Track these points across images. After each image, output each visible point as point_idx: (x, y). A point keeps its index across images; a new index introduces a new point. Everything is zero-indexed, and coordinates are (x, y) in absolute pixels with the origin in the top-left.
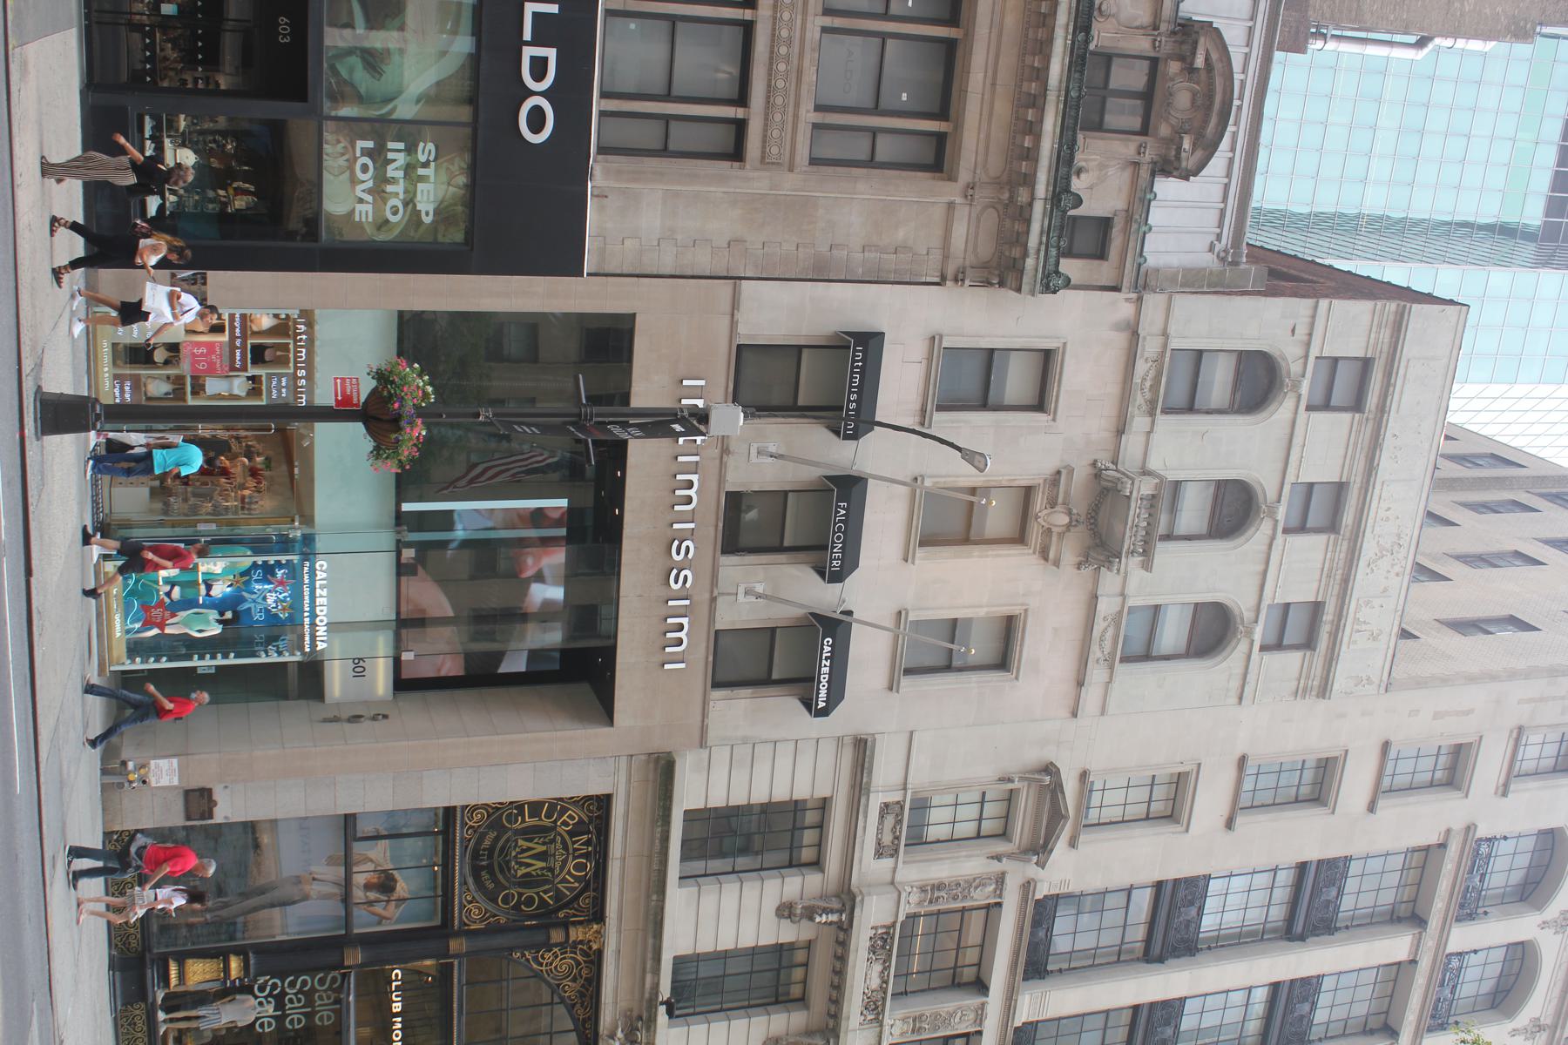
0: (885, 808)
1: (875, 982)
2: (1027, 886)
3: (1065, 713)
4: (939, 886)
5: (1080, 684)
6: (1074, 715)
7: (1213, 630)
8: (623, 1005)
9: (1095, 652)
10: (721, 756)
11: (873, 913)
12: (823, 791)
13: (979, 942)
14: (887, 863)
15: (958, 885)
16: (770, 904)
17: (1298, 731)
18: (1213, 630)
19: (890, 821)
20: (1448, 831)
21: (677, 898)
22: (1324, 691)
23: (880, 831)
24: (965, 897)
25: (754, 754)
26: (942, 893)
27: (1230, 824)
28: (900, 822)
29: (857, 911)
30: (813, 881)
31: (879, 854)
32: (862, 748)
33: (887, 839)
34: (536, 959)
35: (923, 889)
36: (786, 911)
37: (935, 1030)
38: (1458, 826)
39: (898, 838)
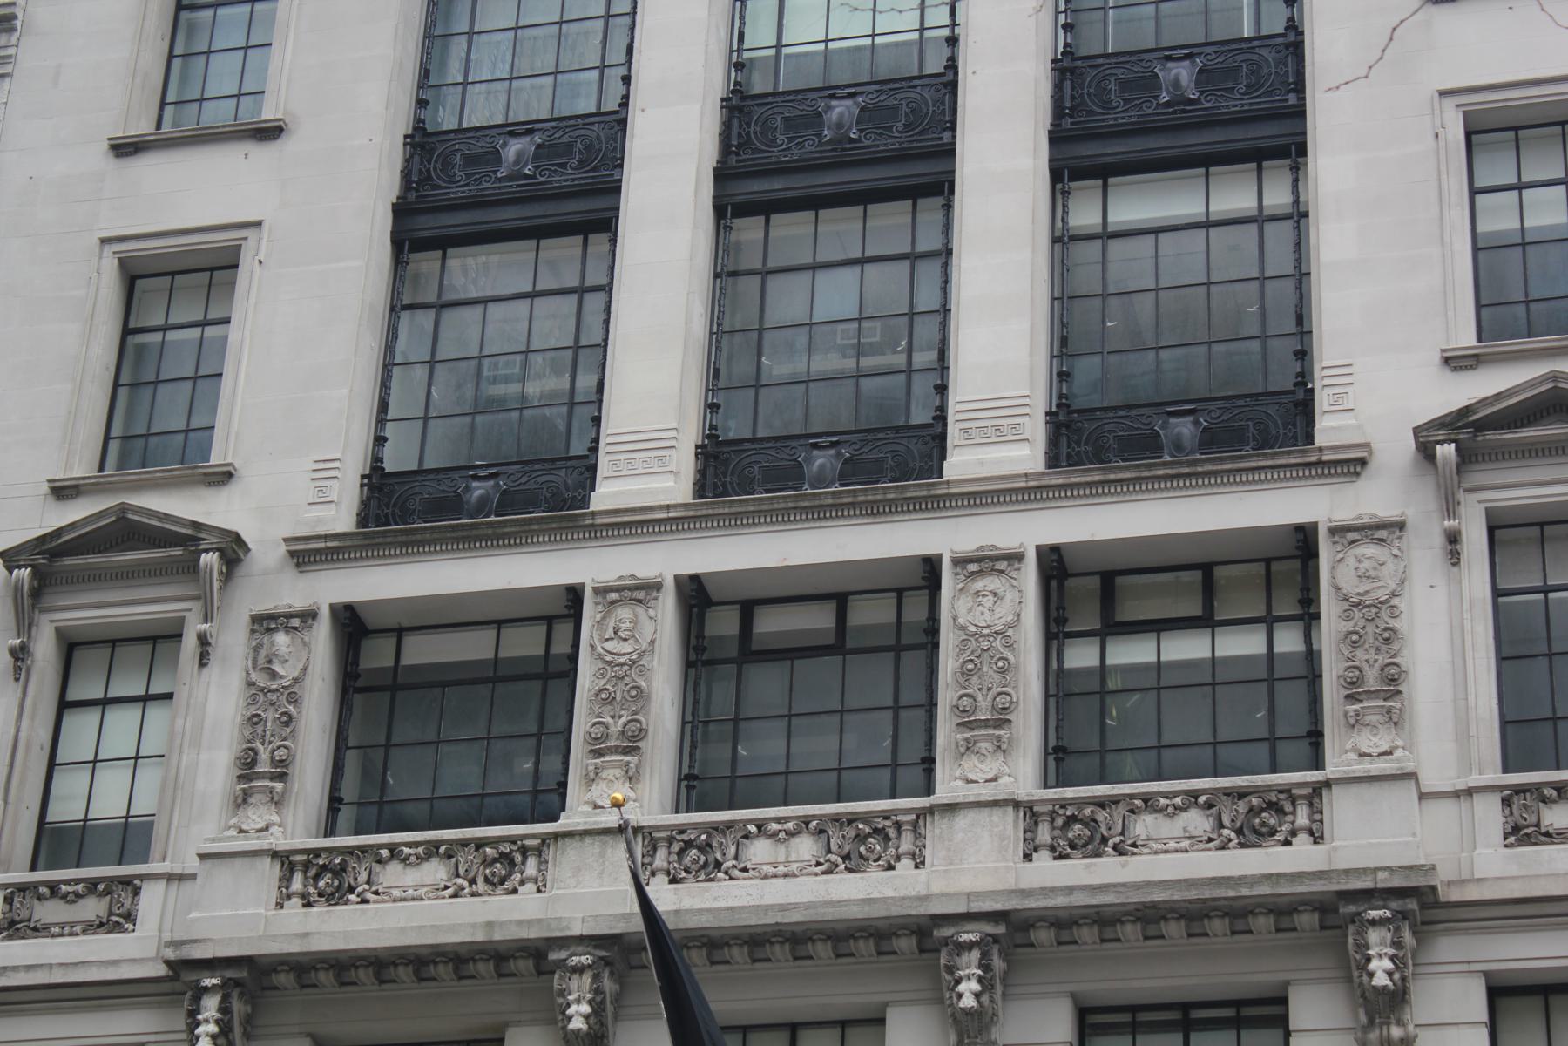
1: (435, 871)
2: (309, 554)
4: (247, 766)
11: (244, 915)
13: (489, 634)
14: (151, 899)
15: (254, 720)
19: (48, 912)
23: (65, 929)
24: (294, 699)
26: (264, 755)
28: (53, 887)
29: (198, 953)
31: (119, 921)
33: (93, 908)
37: (640, 696)
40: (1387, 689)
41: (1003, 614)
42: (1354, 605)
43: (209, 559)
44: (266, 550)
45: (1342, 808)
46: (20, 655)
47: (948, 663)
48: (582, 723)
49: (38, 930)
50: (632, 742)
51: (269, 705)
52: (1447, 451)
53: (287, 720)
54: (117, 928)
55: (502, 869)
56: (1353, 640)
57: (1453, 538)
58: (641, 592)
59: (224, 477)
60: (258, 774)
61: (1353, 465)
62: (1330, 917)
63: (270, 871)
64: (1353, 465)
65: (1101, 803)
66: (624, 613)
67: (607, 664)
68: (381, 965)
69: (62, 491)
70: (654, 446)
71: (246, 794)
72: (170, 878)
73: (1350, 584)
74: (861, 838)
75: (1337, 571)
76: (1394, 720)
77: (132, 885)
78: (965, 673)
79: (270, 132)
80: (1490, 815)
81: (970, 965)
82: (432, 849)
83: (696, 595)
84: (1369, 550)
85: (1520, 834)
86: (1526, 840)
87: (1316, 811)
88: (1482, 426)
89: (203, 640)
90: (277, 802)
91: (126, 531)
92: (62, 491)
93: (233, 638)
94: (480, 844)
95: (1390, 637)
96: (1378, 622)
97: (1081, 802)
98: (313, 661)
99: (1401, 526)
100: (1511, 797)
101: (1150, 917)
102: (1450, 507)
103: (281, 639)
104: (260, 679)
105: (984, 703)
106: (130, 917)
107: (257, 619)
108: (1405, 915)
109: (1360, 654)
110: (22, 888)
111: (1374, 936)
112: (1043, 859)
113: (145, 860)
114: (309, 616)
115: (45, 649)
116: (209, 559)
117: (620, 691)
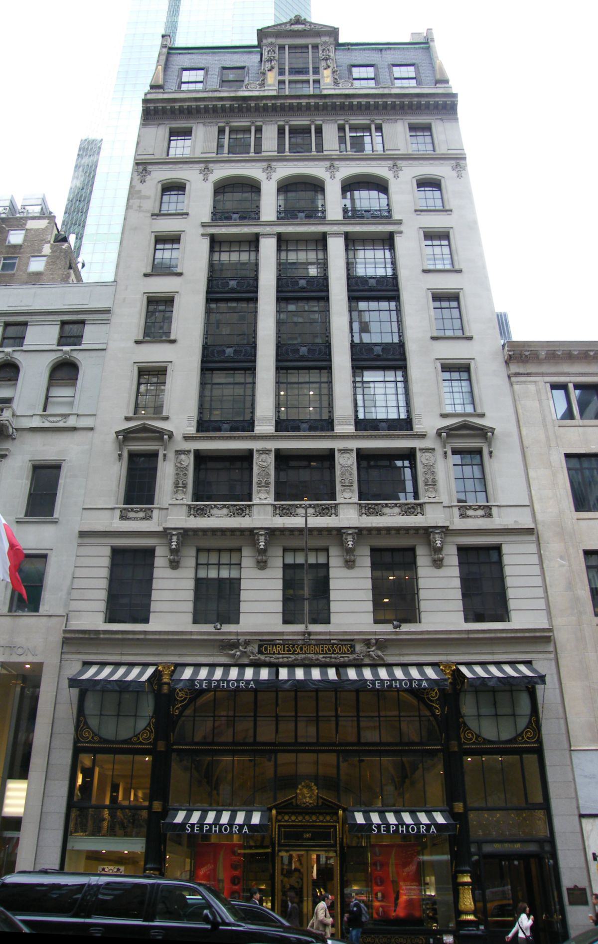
0: (122, 518)
1: (225, 511)
2: (187, 438)
3: (90, 434)
4: (176, 485)
5: (74, 429)
6: (92, 429)
7: (65, 371)
9: (61, 424)
11: (180, 519)
12: (107, 551)
14: (156, 513)
15: (177, 474)
16: (169, 573)
17: (131, 317)
18: (65, 371)
19: (131, 515)
20: (203, 235)
21: (156, 624)
22: (107, 311)
23: (135, 519)
25: (78, 590)
27: (174, 342)
28: (132, 509)
30: (159, 552)
31: (148, 518)
32: (83, 534)
33: (142, 515)
34: (182, 701)
35: (177, 492)
36: (174, 565)
37: (269, 474)
38: (201, 231)
39: (141, 509)
40: (433, 484)
41: (349, 463)
42: (425, 466)
43: (166, 437)
44: (178, 436)
45: (427, 508)
46: (120, 455)
47: (338, 472)
48: (255, 479)
49: (129, 519)
50: (267, 485)
51: (180, 470)
52: (444, 434)
53: (185, 475)
54: (148, 519)
55: (240, 512)
56: (425, 473)
57: (446, 453)
58: (266, 451)
59: (167, 418)
60: (178, 486)
61: (423, 436)
62: (426, 533)
63: (185, 508)
64: (423, 436)
65: (376, 505)
66: (263, 456)
67: (260, 466)
68: (214, 531)
69: (127, 419)
70: (265, 419)
71: (177, 491)
72: (160, 509)
73: (425, 462)
74: (323, 509)
75: (421, 458)
76: (436, 491)
77: (151, 510)
78: (342, 474)
79: (174, 342)
80: (456, 511)
81: (350, 538)
82: (224, 506)
83: (278, 451)
84: (428, 454)
85: (463, 516)
86: (464, 517)
87: (422, 509)
88: (451, 430)
89: (165, 455)
90: (185, 493)
91: (145, 429)
92: (127, 419)
93: (171, 455)
94: (235, 505)
95: (433, 473)
96: (430, 469)
97: (372, 504)
98: (189, 461)
99: (434, 449)
100: (460, 508)
101: (388, 530)
102: (445, 447)
103: (183, 457)
104: (179, 465)
105: (347, 481)
106: (151, 517)
107: (176, 451)
108: (442, 532)
109: (427, 476)
110: (124, 509)
111: (437, 536)
112: (364, 516)
113: (153, 504)
114: (189, 451)
115: (125, 455)
116: (166, 437)
117: (264, 473)
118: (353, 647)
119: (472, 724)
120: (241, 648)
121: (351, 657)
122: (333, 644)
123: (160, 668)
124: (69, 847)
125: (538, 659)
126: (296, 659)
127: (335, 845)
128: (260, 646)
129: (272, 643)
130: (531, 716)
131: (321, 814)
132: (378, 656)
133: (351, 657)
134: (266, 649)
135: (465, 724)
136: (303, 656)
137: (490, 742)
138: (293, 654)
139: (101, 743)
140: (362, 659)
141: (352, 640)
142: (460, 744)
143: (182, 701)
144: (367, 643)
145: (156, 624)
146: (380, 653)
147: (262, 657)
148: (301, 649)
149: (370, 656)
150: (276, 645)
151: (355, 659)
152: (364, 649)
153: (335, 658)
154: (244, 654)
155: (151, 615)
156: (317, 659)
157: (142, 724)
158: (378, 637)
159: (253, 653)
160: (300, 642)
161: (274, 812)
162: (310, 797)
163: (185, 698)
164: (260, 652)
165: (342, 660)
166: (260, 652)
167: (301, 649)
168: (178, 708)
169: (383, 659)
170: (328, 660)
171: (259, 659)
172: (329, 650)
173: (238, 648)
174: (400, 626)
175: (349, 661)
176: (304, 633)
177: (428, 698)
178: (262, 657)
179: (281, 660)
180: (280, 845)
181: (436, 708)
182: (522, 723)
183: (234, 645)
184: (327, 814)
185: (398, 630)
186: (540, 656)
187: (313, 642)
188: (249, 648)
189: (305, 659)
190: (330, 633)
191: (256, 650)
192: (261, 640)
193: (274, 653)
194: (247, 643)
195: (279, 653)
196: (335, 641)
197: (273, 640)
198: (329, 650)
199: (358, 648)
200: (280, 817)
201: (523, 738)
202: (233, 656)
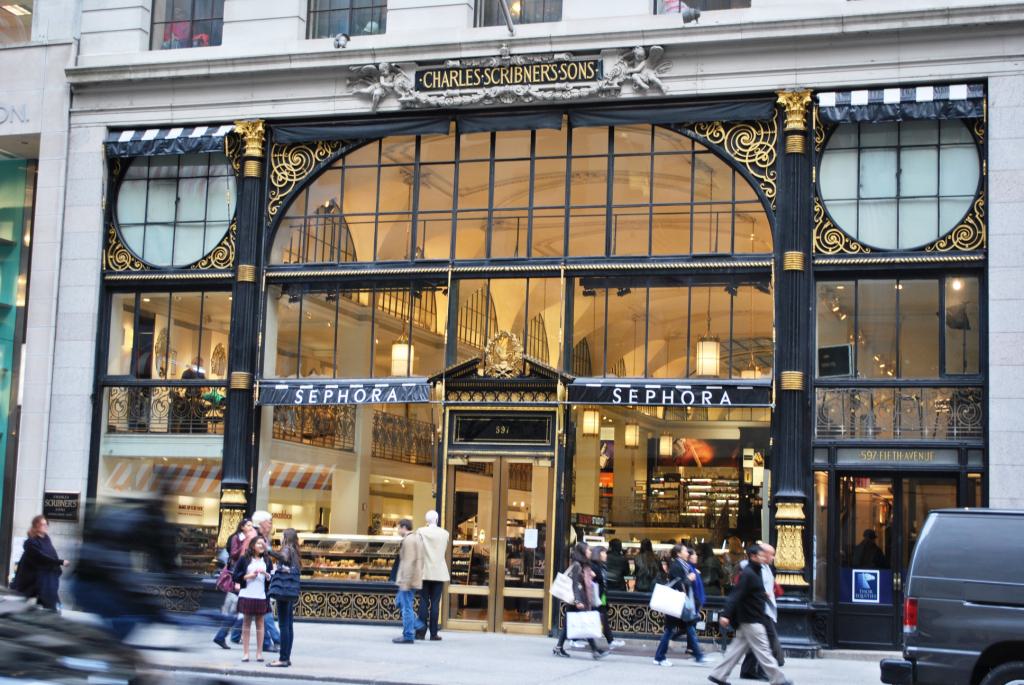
8: (341, 90)
10: (91, 22)
34: (283, 190)
118: (598, 65)
119: (843, 218)
120: (382, 79)
121: (594, 86)
122: (559, 62)
123: (239, 129)
124: (103, 450)
125: (1002, 74)
126: (487, 97)
127: (552, 448)
128: (419, 75)
129: (440, 66)
130: (977, 196)
131: (528, 390)
132: (650, 83)
133: (594, 86)
134: (430, 80)
135: (827, 217)
136: (499, 89)
137: (876, 251)
138: (481, 86)
139: (143, 272)
140: (618, 91)
141: (597, 52)
142: (807, 259)
143: (283, 190)
144: (628, 55)
145: (238, 43)
146: (652, 75)
147: (423, 96)
148: (497, 75)
149: (632, 82)
150: (448, 70)
151: (601, 91)
152: (624, 68)
153: (563, 90)
154: (389, 93)
155: (226, 28)
156: (528, 95)
157: (216, 235)
158: (648, 42)
159: (404, 89)
160: (495, 62)
161: (441, 388)
162: (509, 360)
163: (290, 183)
164: (419, 87)
165: (576, 93)
166: (419, 87)
167: (497, 75)
168: (276, 203)
169: (659, 88)
170: (548, 95)
171: (417, 101)
172: (551, 74)
173: (379, 81)
174: (696, 17)
175: (591, 95)
176: (499, 43)
177: (753, 165)
178: (423, 96)
179: (458, 100)
180: (451, 446)
181: (768, 185)
182: (954, 214)
183: (370, 75)
184: (541, 390)
185: (693, 24)
186: (1008, 66)
187: (519, 60)
188: (399, 80)
189: (503, 95)
190: (550, 40)
191: (411, 83)
192: (420, 63)
193: (445, 88)
194: (394, 70)
195: (454, 87)
196: (563, 56)
197: (442, 62)
198: (551, 74)
199: (611, 66)
200: (453, 399)
201: (950, 243)
202: (368, 97)
